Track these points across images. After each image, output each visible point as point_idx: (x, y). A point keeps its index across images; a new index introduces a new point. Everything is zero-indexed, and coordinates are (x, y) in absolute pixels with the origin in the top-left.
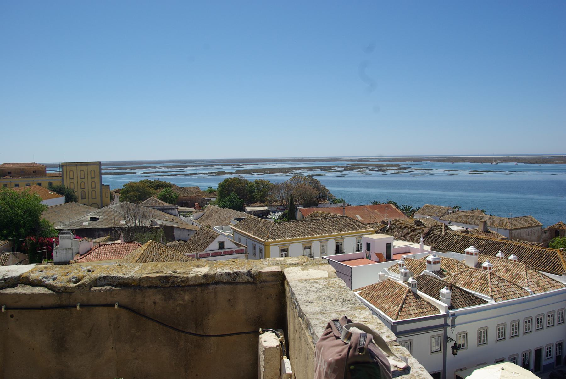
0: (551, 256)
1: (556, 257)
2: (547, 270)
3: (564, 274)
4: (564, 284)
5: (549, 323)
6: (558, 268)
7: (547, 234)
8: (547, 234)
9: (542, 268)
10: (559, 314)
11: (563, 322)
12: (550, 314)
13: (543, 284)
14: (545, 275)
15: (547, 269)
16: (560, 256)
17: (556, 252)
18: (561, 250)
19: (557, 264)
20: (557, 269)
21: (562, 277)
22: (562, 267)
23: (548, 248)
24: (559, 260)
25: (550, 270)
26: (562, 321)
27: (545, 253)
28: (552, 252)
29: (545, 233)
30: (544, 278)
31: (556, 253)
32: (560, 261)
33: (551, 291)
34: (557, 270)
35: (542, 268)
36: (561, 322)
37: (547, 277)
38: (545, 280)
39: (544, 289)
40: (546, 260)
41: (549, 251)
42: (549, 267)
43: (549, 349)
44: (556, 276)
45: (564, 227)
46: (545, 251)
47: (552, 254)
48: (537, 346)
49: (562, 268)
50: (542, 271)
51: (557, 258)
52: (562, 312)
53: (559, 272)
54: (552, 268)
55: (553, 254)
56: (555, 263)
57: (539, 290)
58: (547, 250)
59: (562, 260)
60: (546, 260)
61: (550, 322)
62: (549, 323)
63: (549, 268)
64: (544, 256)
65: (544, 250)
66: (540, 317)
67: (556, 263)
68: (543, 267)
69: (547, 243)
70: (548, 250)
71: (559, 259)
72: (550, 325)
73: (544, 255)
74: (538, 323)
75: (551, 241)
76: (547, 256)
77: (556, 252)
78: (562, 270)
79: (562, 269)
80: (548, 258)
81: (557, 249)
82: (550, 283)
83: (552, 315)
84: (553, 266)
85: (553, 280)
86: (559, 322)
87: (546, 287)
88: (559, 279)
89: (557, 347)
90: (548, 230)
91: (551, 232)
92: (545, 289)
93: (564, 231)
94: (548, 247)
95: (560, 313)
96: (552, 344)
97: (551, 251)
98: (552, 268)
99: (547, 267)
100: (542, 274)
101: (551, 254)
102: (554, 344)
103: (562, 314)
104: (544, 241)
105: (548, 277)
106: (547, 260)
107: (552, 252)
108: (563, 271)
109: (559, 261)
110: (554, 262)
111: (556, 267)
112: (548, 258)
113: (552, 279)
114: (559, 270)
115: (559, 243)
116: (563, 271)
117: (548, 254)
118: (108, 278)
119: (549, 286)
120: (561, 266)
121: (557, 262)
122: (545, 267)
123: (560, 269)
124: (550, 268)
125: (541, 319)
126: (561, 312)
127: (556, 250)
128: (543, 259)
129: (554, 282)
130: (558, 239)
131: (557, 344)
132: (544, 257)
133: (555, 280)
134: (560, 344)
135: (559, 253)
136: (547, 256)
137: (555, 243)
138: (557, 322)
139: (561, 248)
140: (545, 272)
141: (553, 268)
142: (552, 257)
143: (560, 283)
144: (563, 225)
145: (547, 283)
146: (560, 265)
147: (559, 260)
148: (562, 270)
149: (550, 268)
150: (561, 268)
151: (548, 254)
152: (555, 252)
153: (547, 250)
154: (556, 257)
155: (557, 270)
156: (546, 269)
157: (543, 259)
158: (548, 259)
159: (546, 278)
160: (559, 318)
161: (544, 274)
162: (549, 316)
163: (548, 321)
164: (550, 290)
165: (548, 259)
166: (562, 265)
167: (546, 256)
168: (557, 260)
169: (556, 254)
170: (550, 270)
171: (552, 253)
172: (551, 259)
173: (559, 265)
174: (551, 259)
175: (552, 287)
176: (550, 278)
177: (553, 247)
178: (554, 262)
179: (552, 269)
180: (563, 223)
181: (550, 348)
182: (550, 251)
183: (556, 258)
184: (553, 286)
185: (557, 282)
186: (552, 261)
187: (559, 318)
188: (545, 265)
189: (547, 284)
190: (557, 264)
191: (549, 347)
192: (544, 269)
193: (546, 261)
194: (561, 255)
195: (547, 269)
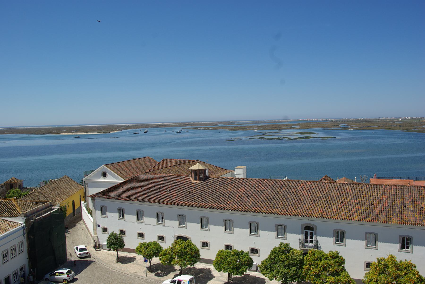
0: (8, 204)
1: (11, 204)
2: (15, 216)
3: (19, 216)
4: (20, 223)
5: (12, 255)
6: (14, 212)
7: (4, 188)
8: (4, 188)
9: (2, 215)
10: (19, 246)
11: (23, 251)
12: (13, 248)
13: (4, 227)
14: (5, 220)
15: (6, 214)
16: (15, 203)
17: (11, 200)
18: (16, 199)
19: (13, 210)
20: (13, 213)
21: (18, 218)
22: (17, 211)
23: (5, 199)
24: (14, 206)
25: (8, 215)
26: (22, 250)
27: (3, 203)
28: (9, 201)
29: (2, 187)
30: (5, 222)
31: (12, 201)
32: (15, 207)
33: (11, 230)
34: (14, 214)
35: (2, 215)
36: (21, 252)
37: (7, 221)
38: (6, 223)
39: (5, 230)
40: (4, 208)
41: (6, 201)
42: (7, 213)
43: (15, 274)
44: (13, 219)
45: (16, 181)
46: (3, 201)
47: (8, 203)
48: (5, 275)
49: (17, 212)
50: (2, 217)
51: (13, 205)
52: (21, 244)
53: (15, 215)
54: (10, 214)
55: (9, 202)
56: (11, 209)
57: (2, 232)
58: (4, 201)
59: (16, 205)
60: (4, 208)
61: (13, 254)
62: (12, 255)
63: (8, 214)
64: (3, 205)
65: (2, 200)
66: (5, 253)
67: (12, 208)
68: (3, 214)
69: (5, 195)
70: (5, 200)
71: (14, 205)
72: (14, 256)
73: (2, 204)
74: (4, 257)
75: (7, 193)
76: (5, 204)
77: (11, 200)
78: (17, 214)
79: (18, 212)
80: (6, 206)
81: (13, 198)
82: (9, 225)
83: (14, 249)
84: (10, 212)
85: (12, 222)
86: (20, 252)
87: (7, 228)
88: (16, 220)
89: (21, 271)
90: (4, 185)
91: (6, 186)
92: (6, 231)
93: (17, 184)
94: (5, 197)
95: (19, 245)
96: (17, 270)
97: (8, 200)
98: (10, 214)
99: (6, 213)
100: (3, 219)
101: (7, 203)
102: (19, 270)
103: (21, 245)
104: (2, 194)
105: (8, 221)
106: (5, 208)
107: (9, 201)
108: (18, 213)
109: (14, 207)
110: (11, 208)
111: (13, 212)
112: (6, 206)
113: (11, 221)
114: (15, 214)
115: (13, 193)
116: (18, 213)
117: (5, 203)
118: (346, 273)
119: (9, 227)
120: (16, 210)
121: (13, 208)
122: (5, 214)
123: (16, 212)
124: (8, 214)
125: (6, 254)
126: (20, 244)
127: (11, 199)
128: (2, 208)
129: (13, 223)
130: (12, 190)
131: (21, 269)
132: (2, 206)
133: (13, 222)
134: (23, 267)
135: (13, 201)
136: (5, 205)
137: (11, 194)
138: (18, 253)
139: (15, 197)
140: (5, 217)
141: (11, 213)
142: (8, 205)
143: (17, 223)
144: (14, 179)
145: (7, 225)
146: (15, 210)
147: (14, 206)
148: (17, 214)
149: (8, 214)
150: (16, 212)
151: (5, 203)
152: (10, 201)
153: (4, 201)
154: (11, 204)
155: (14, 214)
156: (5, 215)
157: (2, 208)
158: (6, 207)
159: (6, 221)
160: (20, 249)
161: (4, 219)
162: (12, 250)
163: (12, 253)
164: (10, 230)
165: (6, 207)
166: (17, 209)
167: (4, 205)
168: (13, 206)
169: (11, 202)
170: (8, 215)
171: (9, 202)
172: (8, 207)
173: (15, 210)
174: (8, 207)
175: (11, 227)
176: (9, 221)
177: (10, 197)
178: (11, 208)
179: (10, 214)
180: (15, 178)
181: (16, 273)
182: (7, 201)
183: (12, 205)
184: (12, 226)
185: (15, 223)
186: (9, 208)
187: (20, 249)
188: (4, 212)
189: (7, 226)
190: (13, 210)
191: (15, 273)
192: (3, 215)
193: (5, 209)
194: (15, 202)
195: (6, 214)
